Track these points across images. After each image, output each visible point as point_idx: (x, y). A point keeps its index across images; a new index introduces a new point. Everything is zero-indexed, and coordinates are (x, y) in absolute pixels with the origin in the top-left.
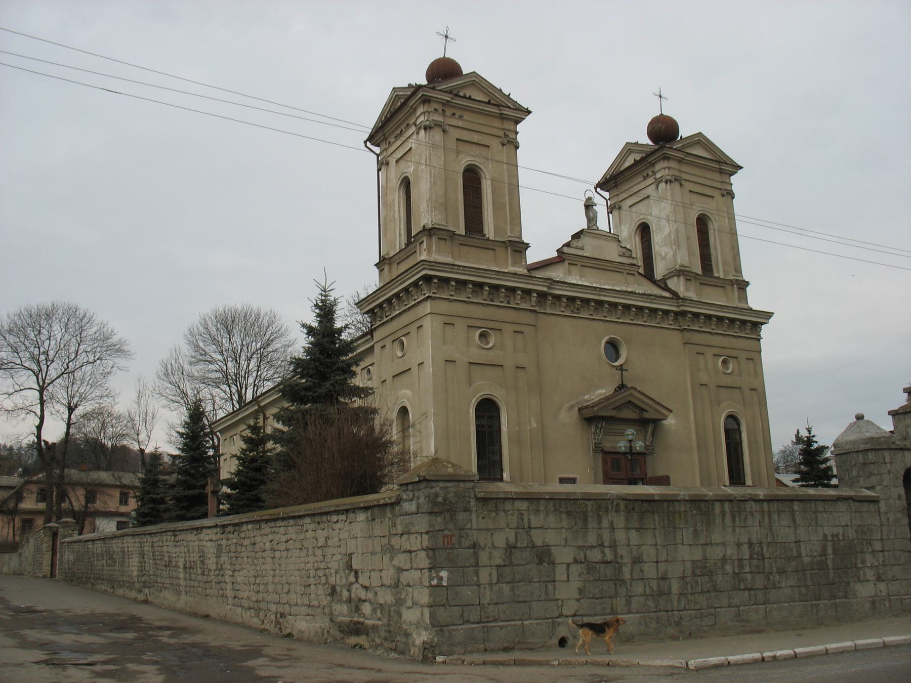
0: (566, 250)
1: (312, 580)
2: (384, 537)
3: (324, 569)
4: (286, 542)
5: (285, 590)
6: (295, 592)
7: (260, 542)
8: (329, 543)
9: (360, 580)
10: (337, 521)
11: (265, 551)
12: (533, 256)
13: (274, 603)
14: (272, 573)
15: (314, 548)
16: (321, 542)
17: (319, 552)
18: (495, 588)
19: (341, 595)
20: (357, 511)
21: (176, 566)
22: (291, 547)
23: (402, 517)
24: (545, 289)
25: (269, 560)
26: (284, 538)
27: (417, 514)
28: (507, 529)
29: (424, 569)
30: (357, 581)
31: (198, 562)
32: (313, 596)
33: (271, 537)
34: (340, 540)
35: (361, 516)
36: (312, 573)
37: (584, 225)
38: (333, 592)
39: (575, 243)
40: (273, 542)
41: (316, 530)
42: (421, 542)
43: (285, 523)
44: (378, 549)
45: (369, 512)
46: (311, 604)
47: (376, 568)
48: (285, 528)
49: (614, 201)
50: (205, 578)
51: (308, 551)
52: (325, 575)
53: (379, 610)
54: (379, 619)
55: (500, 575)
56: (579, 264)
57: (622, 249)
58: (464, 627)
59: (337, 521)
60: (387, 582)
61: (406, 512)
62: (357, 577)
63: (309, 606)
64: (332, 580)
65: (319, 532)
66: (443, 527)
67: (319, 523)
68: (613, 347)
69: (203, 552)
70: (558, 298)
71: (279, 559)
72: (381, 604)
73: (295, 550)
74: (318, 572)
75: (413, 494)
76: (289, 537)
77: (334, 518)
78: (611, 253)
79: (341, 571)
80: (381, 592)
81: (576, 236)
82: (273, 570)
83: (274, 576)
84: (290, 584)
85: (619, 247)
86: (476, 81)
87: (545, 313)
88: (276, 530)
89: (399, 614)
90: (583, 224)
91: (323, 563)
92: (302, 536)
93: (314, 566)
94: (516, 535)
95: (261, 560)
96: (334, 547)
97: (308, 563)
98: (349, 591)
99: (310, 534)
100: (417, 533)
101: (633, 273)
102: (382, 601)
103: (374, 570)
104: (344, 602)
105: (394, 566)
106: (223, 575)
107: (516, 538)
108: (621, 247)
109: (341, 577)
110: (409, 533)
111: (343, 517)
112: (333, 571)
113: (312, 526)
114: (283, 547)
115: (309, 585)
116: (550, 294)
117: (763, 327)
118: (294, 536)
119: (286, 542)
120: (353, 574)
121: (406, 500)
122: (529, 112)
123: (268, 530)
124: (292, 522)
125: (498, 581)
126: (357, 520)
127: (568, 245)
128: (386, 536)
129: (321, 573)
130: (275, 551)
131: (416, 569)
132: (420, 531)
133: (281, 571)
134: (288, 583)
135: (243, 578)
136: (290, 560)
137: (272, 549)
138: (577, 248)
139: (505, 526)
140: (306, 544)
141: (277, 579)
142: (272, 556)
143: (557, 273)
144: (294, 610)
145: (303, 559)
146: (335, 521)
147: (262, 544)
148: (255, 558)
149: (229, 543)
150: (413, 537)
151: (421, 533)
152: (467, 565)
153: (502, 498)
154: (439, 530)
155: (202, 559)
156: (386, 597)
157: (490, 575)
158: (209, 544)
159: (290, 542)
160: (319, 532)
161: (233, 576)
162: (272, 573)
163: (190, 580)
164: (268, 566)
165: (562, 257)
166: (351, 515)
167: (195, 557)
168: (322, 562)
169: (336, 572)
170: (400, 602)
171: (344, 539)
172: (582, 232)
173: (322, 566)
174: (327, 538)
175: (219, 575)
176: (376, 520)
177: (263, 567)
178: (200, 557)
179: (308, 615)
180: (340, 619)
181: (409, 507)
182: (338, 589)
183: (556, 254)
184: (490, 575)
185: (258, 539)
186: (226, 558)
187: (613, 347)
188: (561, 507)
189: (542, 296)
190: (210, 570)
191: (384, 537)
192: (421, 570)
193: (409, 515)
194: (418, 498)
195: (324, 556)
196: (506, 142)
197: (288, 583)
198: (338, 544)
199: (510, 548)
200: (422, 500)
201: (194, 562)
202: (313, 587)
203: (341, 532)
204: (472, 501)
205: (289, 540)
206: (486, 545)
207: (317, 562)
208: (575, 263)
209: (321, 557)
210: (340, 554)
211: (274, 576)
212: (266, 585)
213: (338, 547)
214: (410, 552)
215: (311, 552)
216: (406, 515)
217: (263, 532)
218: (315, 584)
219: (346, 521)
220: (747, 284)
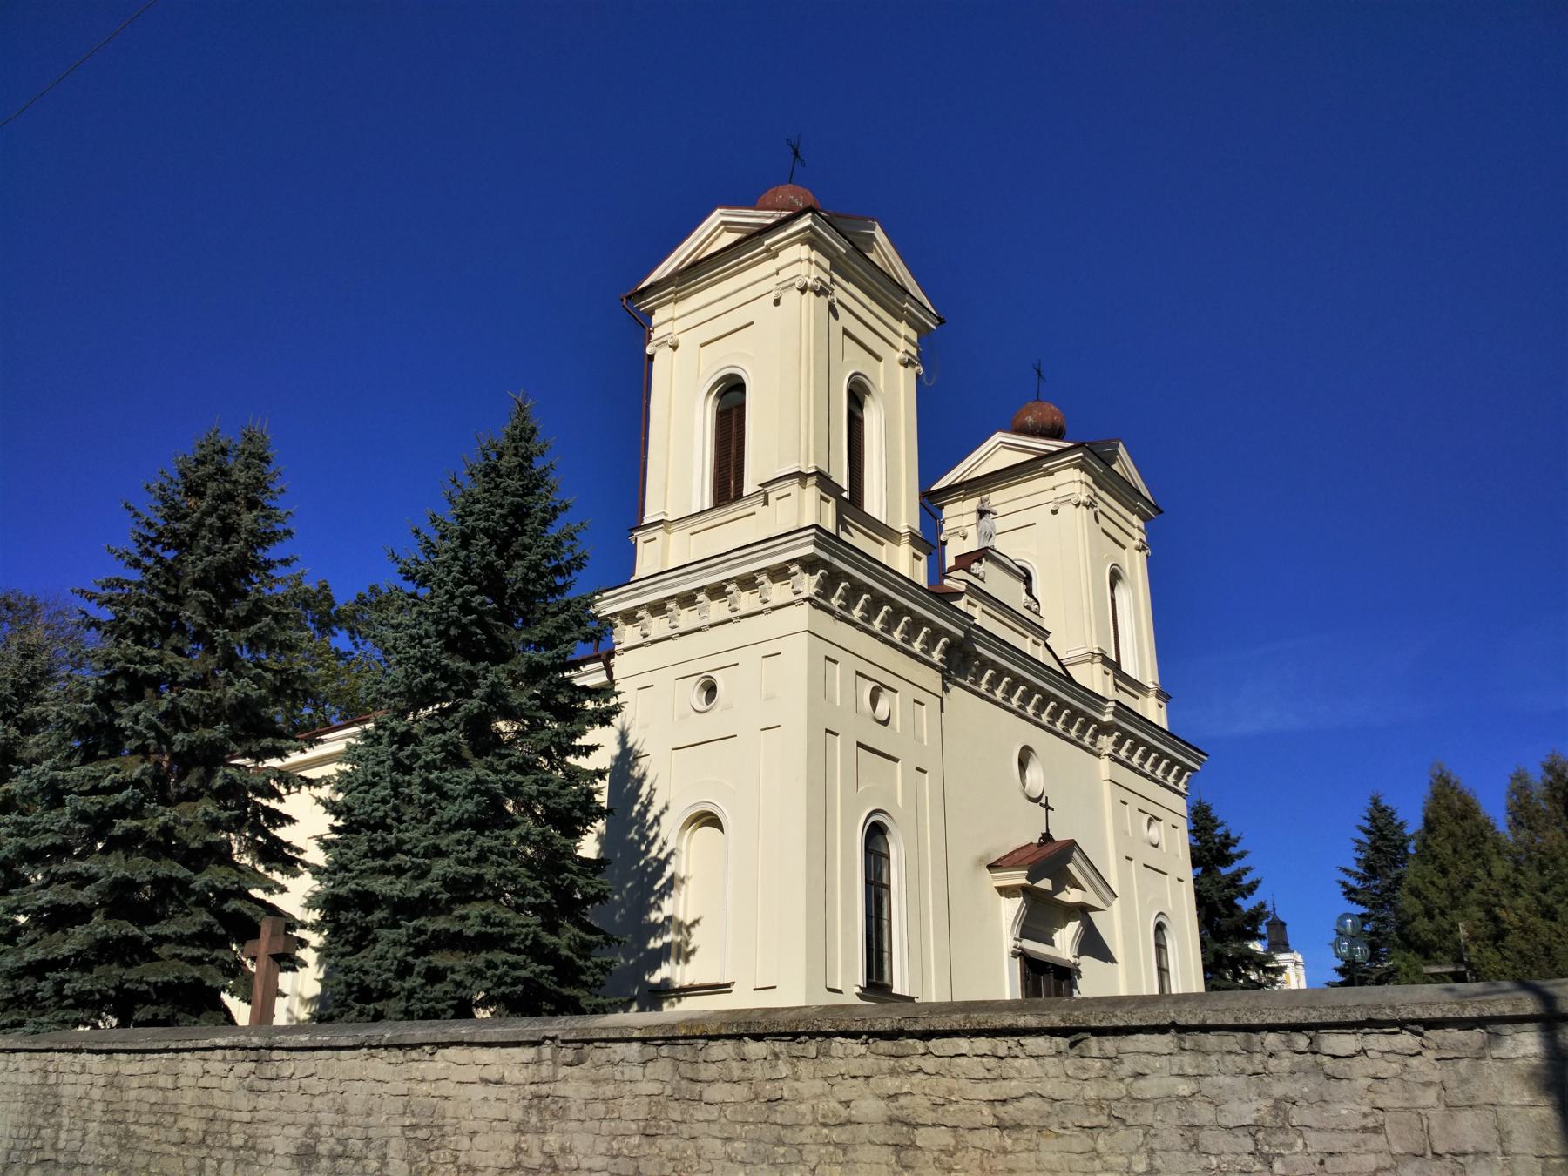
26: (983, 1091)
33: (891, 1084)
88: (929, 1064)
113: (1188, 1062)
123: (886, 1063)
138: (976, 576)
145: (1122, 1160)
147: (834, 1104)
148: (780, 1142)
198: (1370, 1122)
203: (1382, 1087)
213: (1365, 1130)
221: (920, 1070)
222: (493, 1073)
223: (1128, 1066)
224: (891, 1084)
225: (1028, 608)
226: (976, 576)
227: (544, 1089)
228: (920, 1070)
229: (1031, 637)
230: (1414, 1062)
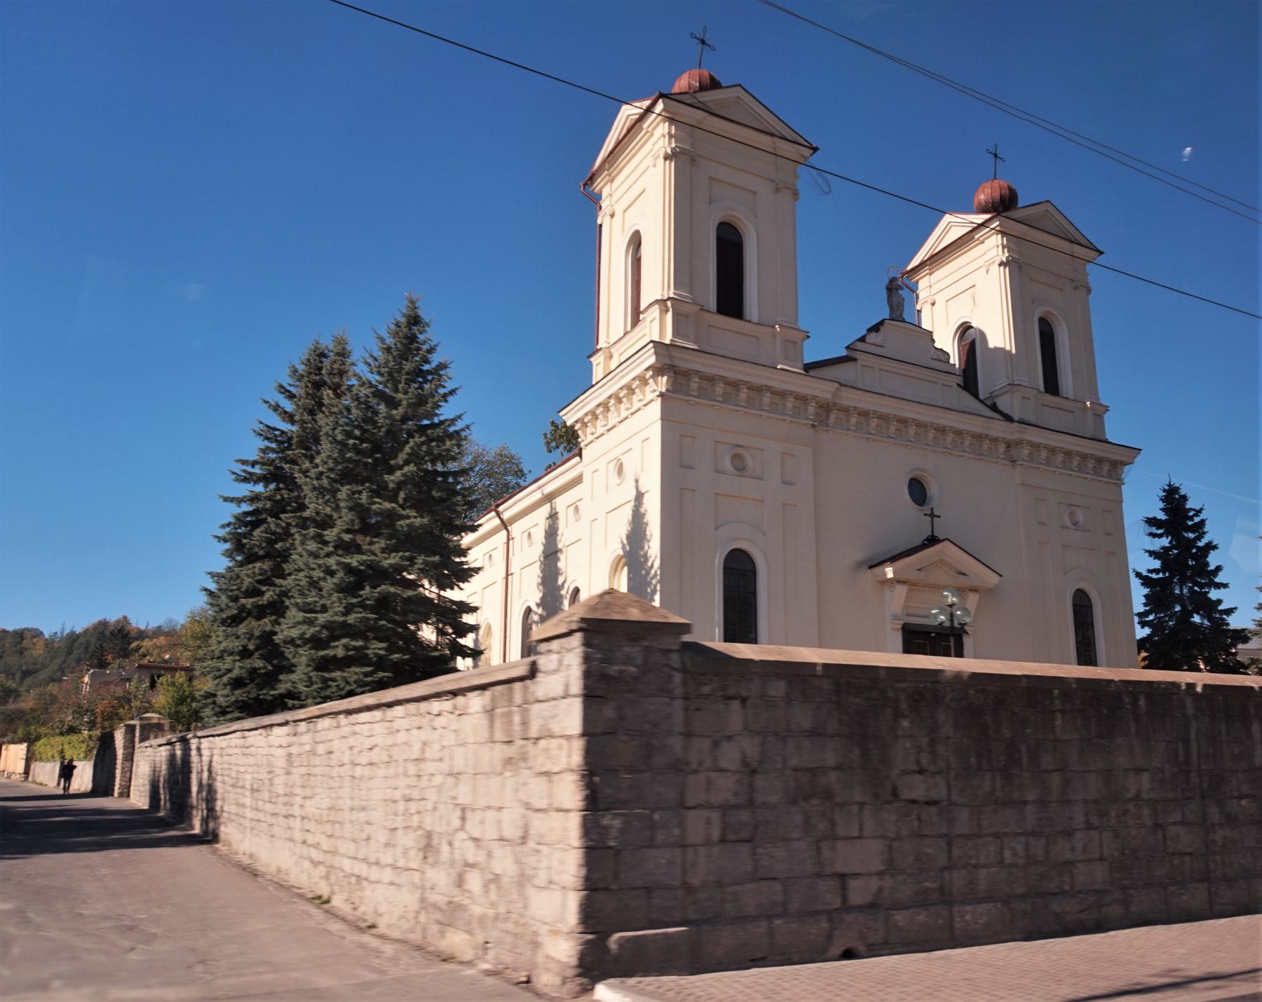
8: (428, 755)
9: (469, 825)
21: (243, 787)
30: (462, 828)
55: (725, 827)
68: (918, 490)
80: (498, 850)
99: (402, 737)
101: (951, 384)
117: (1126, 468)
123: (346, 730)
125: (723, 840)
129: (413, 807)
140: (395, 753)
146: (437, 713)
157: (708, 822)
159: (376, 750)
160: (415, 732)
174: (425, 743)
184: (708, 822)
185: (336, 744)
187: (918, 490)
220: (1106, 409)
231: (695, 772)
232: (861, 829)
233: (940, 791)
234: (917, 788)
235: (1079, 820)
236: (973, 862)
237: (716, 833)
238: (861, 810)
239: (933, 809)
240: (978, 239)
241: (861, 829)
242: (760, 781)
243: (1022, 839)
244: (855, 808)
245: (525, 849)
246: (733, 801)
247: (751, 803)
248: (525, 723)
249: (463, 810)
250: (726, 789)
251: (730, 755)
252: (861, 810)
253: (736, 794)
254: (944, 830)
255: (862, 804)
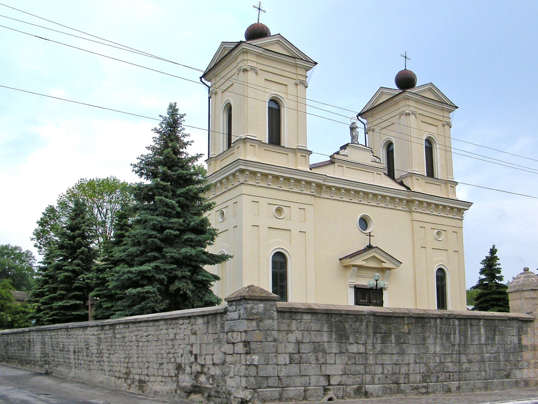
0: (336, 156)
1: (164, 360)
2: (215, 334)
3: (174, 353)
4: (147, 336)
5: (146, 366)
6: (152, 368)
7: (129, 336)
8: (177, 337)
9: (199, 360)
10: (183, 324)
11: (132, 342)
12: (314, 159)
13: (138, 374)
14: (136, 355)
15: (166, 340)
16: (172, 336)
17: (170, 343)
18: (287, 367)
19: (184, 370)
20: (196, 317)
22: (151, 339)
23: (228, 322)
24: (321, 182)
25: (134, 347)
26: (145, 334)
27: (238, 320)
28: (297, 331)
29: (242, 354)
31: (84, 349)
32: (165, 370)
33: (136, 333)
34: (185, 335)
35: (200, 321)
36: (165, 355)
37: (348, 140)
38: (179, 367)
39: (342, 152)
40: (137, 337)
41: (168, 329)
42: (241, 338)
43: (146, 324)
44: (212, 341)
45: (205, 318)
46: (164, 375)
47: (209, 353)
48: (146, 327)
49: (369, 126)
50: (89, 359)
51: (162, 342)
52: (173, 357)
53: (211, 379)
54: (210, 384)
55: (291, 359)
56: (345, 166)
57: (374, 158)
58: (267, 389)
59: (183, 324)
60: (217, 361)
61: (231, 318)
62: (196, 358)
63: (162, 376)
64: (179, 360)
65: (170, 330)
66: (255, 328)
67: (170, 324)
68: (364, 222)
69: (88, 342)
70: (329, 187)
71: (142, 347)
72: (212, 375)
73: (153, 342)
74: (169, 355)
75: (236, 308)
76: (149, 333)
77: (181, 322)
78: (366, 158)
79: (185, 355)
81: (343, 147)
82: (137, 354)
83: (138, 357)
84: (149, 363)
85: (372, 156)
86: (281, 40)
87: (320, 197)
88: (140, 328)
89: (225, 381)
90: (348, 140)
91: (173, 350)
92: (158, 333)
93: (166, 352)
94: (303, 335)
95: (129, 348)
96: (180, 340)
97: (162, 349)
98: (191, 367)
99: (164, 331)
100: (238, 332)
102: (213, 373)
103: (208, 354)
104: (187, 374)
105: (222, 352)
106: (102, 357)
107: (303, 337)
108: (374, 156)
109: (185, 359)
110: (233, 331)
111: (187, 321)
112: (179, 355)
113: (165, 327)
114: (144, 339)
115: (163, 363)
116: (324, 185)
118: (152, 333)
119: (147, 336)
120: (193, 356)
121: (231, 311)
122: (316, 63)
123: (135, 329)
124: (151, 324)
126: (197, 323)
127: (338, 153)
128: (216, 333)
129: (171, 356)
130: (139, 342)
131: (237, 354)
132: (240, 331)
133: (143, 354)
134: (147, 362)
135: (116, 359)
136: (149, 348)
137: (136, 341)
138: (343, 155)
139: (296, 329)
140: (161, 337)
141: (140, 360)
142: (137, 345)
143: (329, 171)
144: (152, 379)
148: (125, 346)
149: (106, 336)
150: (235, 334)
151: (241, 332)
152: (270, 352)
153: (294, 312)
154: (253, 330)
155: (86, 346)
156: (215, 371)
157: (285, 359)
158: (92, 337)
161: (109, 357)
162: (136, 355)
163: (79, 360)
164: (134, 351)
165: (332, 161)
166: (192, 320)
167: (83, 345)
168: (172, 349)
169: (182, 356)
170: (224, 375)
171: (187, 335)
172: (347, 145)
173: (172, 351)
175: (99, 356)
176: (210, 323)
177: (131, 352)
178: (86, 345)
179: (162, 382)
180: (184, 384)
181: (231, 315)
182: (183, 366)
183: (329, 159)
184: (285, 359)
185: (127, 334)
186: (104, 346)
187: (364, 222)
188: (331, 318)
189: (319, 186)
190: (93, 354)
191: (215, 334)
192: (240, 354)
193: (233, 320)
194: (239, 310)
195: (173, 345)
196: (299, 83)
197: (147, 362)
199: (299, 343)
200: (242, 311)
201: (81, 348)
202: (165, 364)
203: (185, 330)
204: (275, 314)
205: (149, 335)
206: (283, 340)
207: (169, 349)
208: (342, 165)
209: (172, 346)
210: (185, 344)
211: (138, 357)
212: (133, 363)
213: (183, 339)
214: (233, 343)
215: (164, 342)
216: (231, 320)
217: (130, 330)
218: (167, 363)
219: (189, 324)
221: (139, 330)
222: (93, 333)
223: (160, 328)
224: (136, 333)
225: (375, 162)
226: (343, 155)
227: (99, 336)
228: (139, 330)
229: (375, 172)
230: (189, 325)
231: (281, 343)
232: (335, 362)
233: (362, 349)
234: (353, 348)
235: (412, 361)
236: (373, 373)
237: (288, 362)
238: (335, 356)
239: (360, 355)
240: (396, 101)
241: (335, 362)
242: (303, 346)
243: (391, 366)
244: (333, 355)
245: (224, 366)
246: (293, 352)
247: (299, 352)
248: (223, 327)
249: (196, 356)
250: (291, 348)
251: (292, 337)
252: (335, 356)
253: (294, 350)
254: (364, 362)
255: (336, 354)
